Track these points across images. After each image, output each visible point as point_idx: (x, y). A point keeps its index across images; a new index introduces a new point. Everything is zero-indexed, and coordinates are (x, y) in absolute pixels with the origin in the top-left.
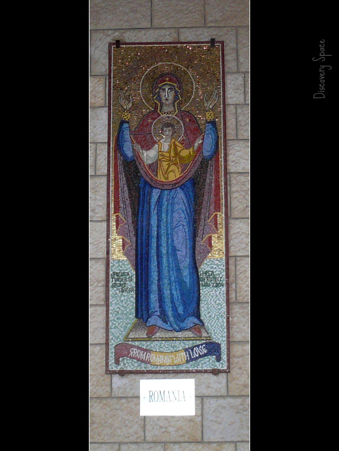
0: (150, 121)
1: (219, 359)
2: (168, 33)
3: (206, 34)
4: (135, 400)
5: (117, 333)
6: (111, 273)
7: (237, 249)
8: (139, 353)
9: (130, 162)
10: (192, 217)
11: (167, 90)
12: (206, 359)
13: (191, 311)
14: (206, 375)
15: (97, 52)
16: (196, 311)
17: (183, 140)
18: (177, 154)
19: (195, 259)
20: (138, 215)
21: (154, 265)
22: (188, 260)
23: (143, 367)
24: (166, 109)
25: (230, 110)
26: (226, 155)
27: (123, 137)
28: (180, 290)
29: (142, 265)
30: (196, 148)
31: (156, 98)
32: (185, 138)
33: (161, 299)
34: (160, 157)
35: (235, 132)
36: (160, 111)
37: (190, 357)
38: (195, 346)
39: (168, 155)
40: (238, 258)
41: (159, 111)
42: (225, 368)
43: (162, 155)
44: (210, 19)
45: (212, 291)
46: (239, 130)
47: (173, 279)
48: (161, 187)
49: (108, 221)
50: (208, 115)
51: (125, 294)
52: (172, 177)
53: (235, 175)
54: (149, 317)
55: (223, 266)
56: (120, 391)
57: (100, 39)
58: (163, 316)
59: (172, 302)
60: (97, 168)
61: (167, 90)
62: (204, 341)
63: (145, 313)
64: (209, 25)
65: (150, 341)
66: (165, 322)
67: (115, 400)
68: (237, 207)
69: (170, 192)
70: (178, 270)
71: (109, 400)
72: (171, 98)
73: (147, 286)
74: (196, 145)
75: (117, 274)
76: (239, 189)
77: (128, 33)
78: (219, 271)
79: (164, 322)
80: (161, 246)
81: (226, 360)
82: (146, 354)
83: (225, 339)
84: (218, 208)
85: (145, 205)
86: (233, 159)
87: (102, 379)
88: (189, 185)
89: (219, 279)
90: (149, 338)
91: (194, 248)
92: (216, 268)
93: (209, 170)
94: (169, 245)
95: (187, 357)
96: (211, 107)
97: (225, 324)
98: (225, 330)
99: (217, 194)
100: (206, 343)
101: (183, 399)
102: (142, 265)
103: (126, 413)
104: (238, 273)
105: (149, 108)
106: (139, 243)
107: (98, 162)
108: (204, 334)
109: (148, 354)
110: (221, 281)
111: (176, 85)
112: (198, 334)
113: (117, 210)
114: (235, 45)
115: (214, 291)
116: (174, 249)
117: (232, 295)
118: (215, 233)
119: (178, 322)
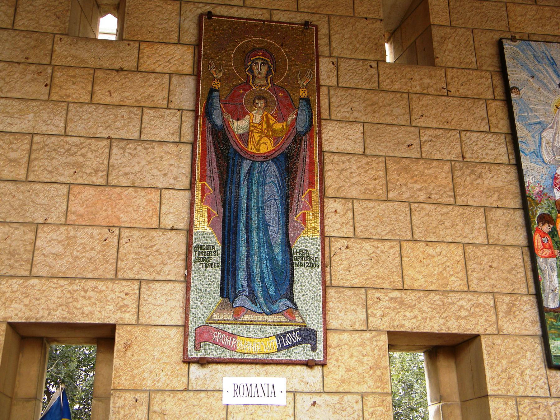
0: (241, 92)
1: (314, 348)
2: (261, 13)
3: (299, 18)
4: (217, 394)
5: (198, 314)
6: (194, 245)
7: (332, 229)
8: (223, 338)
9: (220, 131)
10: (285, 191)
11: (260, 64)
12: (300, 348)
13: (283, 292)
14: (299, 368)
15: (186, 22)
16: (289, 293)
17: (276, 114)
18: (269, 126)
19: (288, 236)
20: (226, 184)
21: (242, 238)
22: (280, 237)
23: (227, 355)
24: (257, 81)
25: (324, 91)
26: (320, 133)
27: (212, 105)
28: (271, 269)
29: (229, 238)
30: (289, 123)
31: (249, 70)
32: (278, 112)
33: (250, 277)
34: (252, 128)
35: (328, 112)
36: (253, 83)
37: (282, 345)
38: (288, 332)
39: (260, 127)
40: (332, 239)
41: (251, 83)
42: (322, 359)
43: (253, 126)
44: (302, 5)
45: (306, 271)
46: (332, 111)
47: (263, 256)
48: (251, 158)
49: (192, 187)
50: (301, 92)
51: (209, 269)
52: (264, 149)
53: (328, 155)
54: (236, 296)
55: (319, 245)
56: (199, 383)
57: (191, 10)
58: (252, 296)
59: (263, 281)
60: (182, 134)
61: (260, 64)
62: (298, 327)
63: (231, 291)
64: (302, 10)
65: (237, 324)
66: (254, 302)
67: (192, 393)
68: (331, 186)
69: (261, 165)
70: (270, 246)
71: (185, 393)
72: (264, 70)
73: (235, 262)
74: (290, 119)
75: (201, 247)
76: (332, 168)
77: (220, 7)
78: (314, 250)
79: (253, 303)
80: (251, 219)
81: (322, 349)
82: (232, 340)
83: (321, 326)
84: (312, 184)
85: (235, 176)
86: (326, 138)
87: (178, 367)
88: (282, 159)
89: (314, 259)
90: (236, 321)
91: (286, 224)
92: (310, 247)
93: (303, 146)
94: (260, 219)
95: (279, 345)
96: (305, 84)
97: (321, 309)
98: (321, 316)
99: (312, 171)
100: (300, 330)
101: (273, 394)
102: (229, 238)
103: (205, 411)
104: (332, 255)
105: (240, 80)
106: (227, 215)
107: (183, 128)
108: (298, 319)
109: (234, 339)
110: (316, 260)
111: (269, 60)
112: (290, 318)
113: (202, 179)
114: (327, 32)
115: (308, 271)
116: (266, 224)
117: (328, 278)
118: (309, 209)
119: (269, 304)
